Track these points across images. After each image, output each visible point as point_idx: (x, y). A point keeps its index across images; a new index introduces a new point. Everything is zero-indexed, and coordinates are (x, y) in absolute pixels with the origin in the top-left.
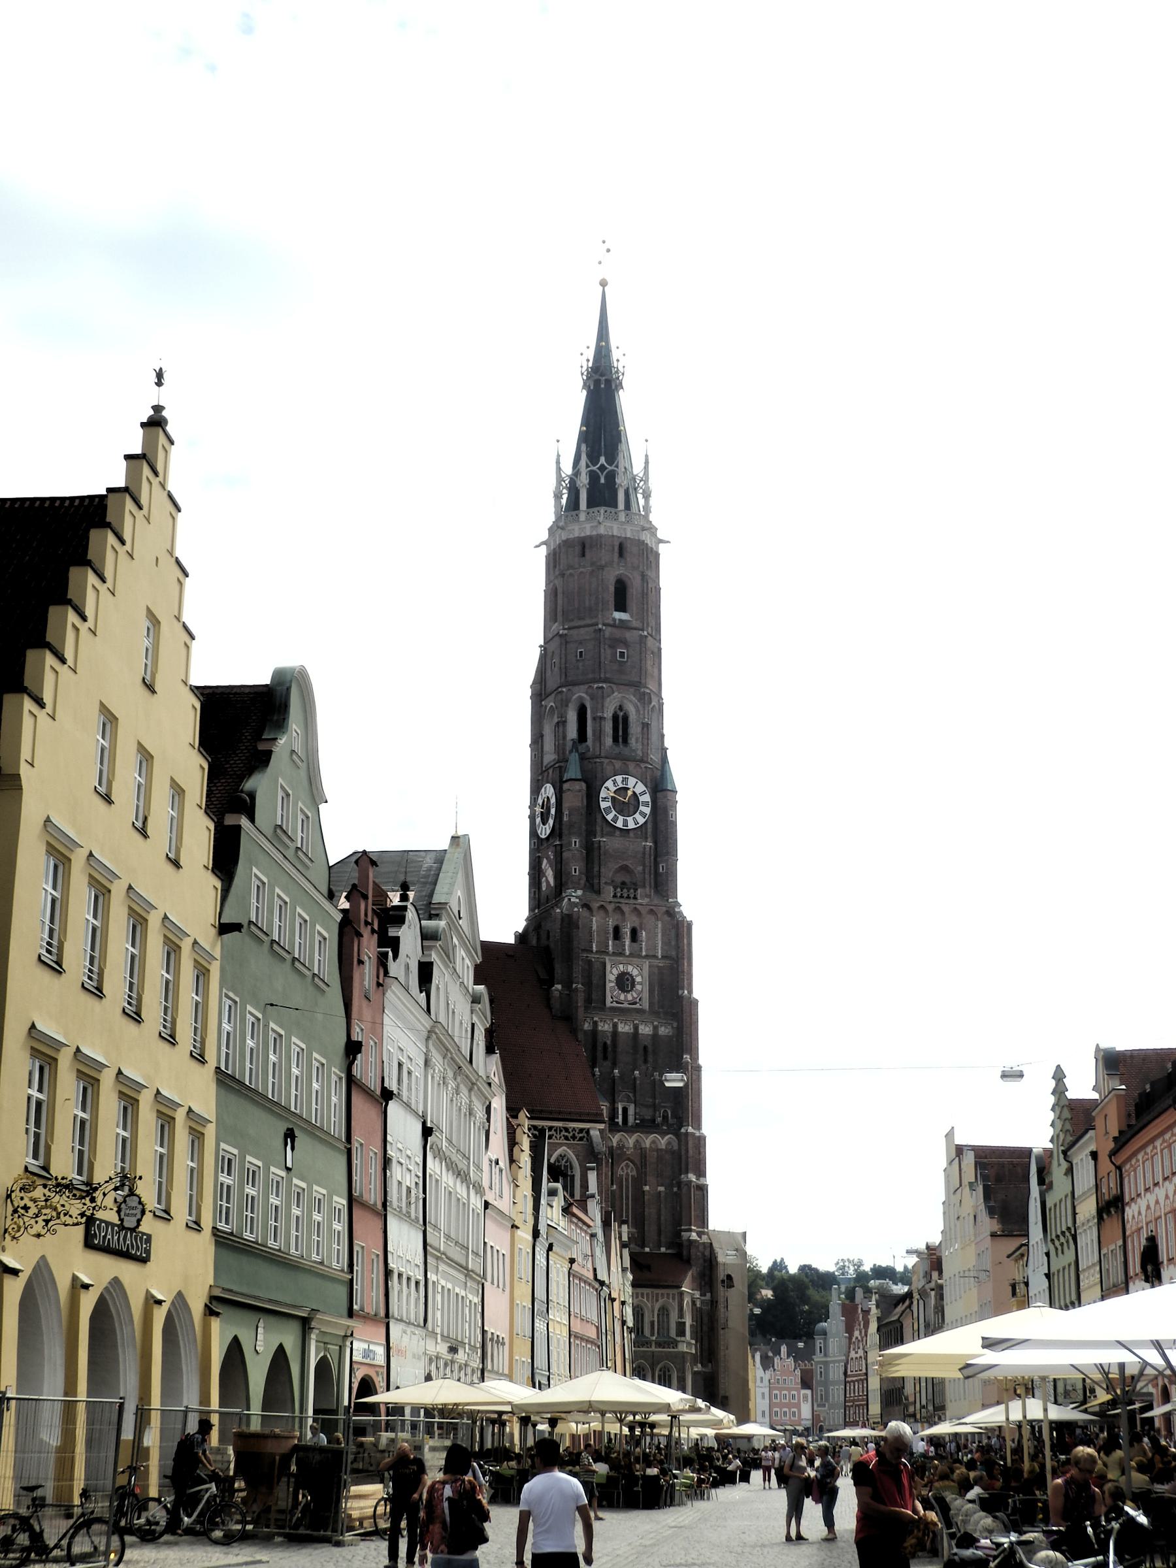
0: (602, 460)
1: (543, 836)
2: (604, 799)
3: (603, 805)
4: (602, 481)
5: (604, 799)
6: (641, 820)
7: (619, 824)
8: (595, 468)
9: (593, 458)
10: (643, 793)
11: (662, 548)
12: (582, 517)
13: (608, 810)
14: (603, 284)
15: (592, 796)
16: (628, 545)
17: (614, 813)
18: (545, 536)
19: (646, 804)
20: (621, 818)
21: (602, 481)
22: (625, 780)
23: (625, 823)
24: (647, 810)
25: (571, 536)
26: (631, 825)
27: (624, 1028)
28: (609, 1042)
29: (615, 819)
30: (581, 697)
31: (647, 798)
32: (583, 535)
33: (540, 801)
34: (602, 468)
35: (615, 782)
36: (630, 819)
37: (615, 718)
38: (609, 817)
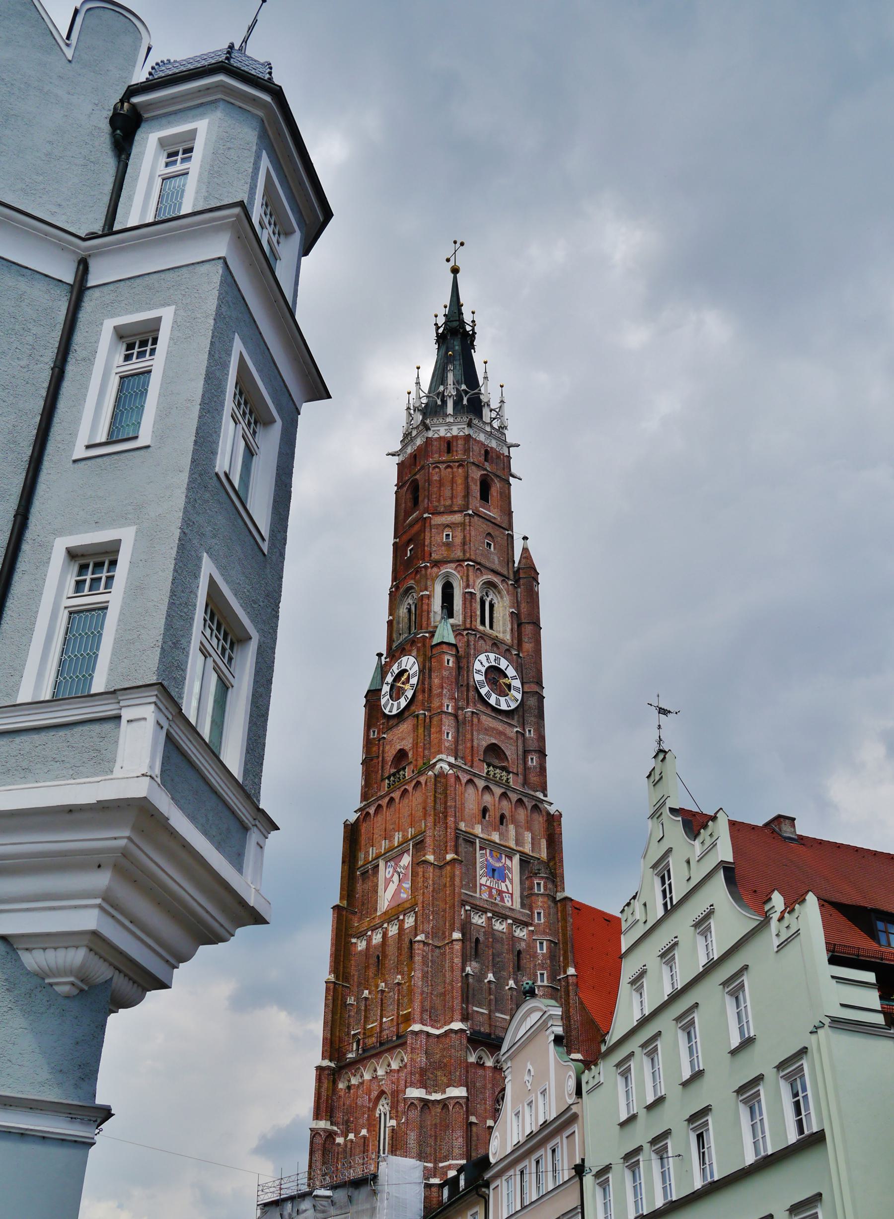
0: (464, 387)
1: (395, 712)
2: (478, 672)
4: (465, 402)
6: (513, 706)
7: (492, 701)
9: (457, 383)
10: (514, 678)
11: (511, 480)
12: (450, 419)
18: (399, 447)
21: (465, 402)
25: (436, 436)
26: (504, 707)
27: (500, 926)
28: (482, 939)
29: (488, 695)
30: (447, 575)
31: (517, 683)
32: (449, 435)
33: (389, 679)
34: (466, 393)
36: (502, 699)
38: (483, 691)
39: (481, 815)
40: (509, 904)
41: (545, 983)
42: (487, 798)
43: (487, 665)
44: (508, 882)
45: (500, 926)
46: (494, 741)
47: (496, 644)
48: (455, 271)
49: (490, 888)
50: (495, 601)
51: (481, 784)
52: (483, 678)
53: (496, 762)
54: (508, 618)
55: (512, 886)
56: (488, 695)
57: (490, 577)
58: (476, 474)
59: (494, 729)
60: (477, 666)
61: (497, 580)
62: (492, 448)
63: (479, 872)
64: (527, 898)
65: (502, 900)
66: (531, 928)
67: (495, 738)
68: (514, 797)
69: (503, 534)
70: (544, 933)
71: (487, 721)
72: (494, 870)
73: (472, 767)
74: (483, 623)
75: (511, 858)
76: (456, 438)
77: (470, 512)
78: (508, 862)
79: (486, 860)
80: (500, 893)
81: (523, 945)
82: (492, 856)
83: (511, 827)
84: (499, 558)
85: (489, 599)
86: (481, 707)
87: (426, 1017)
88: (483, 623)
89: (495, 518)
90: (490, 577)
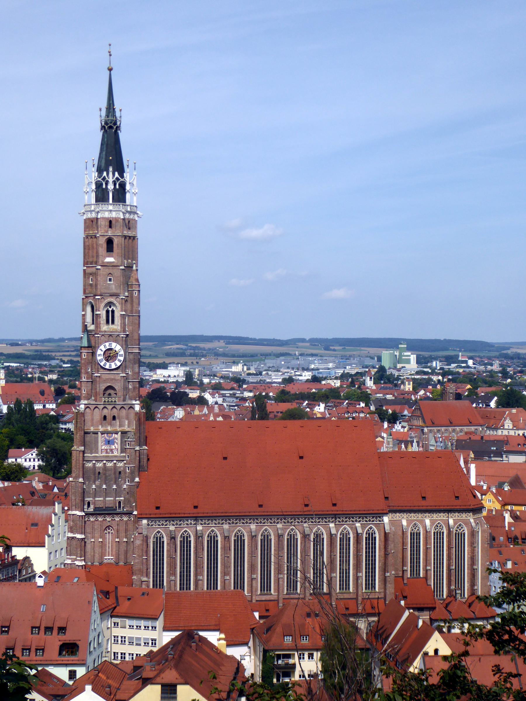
2: (99, 355)
3: (99, 358)
5: (99, 355)
6: (119, 364)
7: (107, 367)
8: (100, 179)
13: (101, 361)
14: (110, 70)
15: (93, 354)
16: (113, 222)
17: (104, 361)
19: (121, 356)
20: (108, 364)
22: (110, 345)
23: (110, 366)
24: (122, 358)
27: (110, 465)
31: (122, 352)
35: (105, 346)
38: (102, 364)
39: (103, 419)
40: (115, 454)
41: (129, 484)
42: (105, 411)
43: (104, 350)
44: (116, 445)
45: (110, 465)
46: (109, 385)
47: (111, 337)
48: (110, 70)
49: (107, 450)
50: (114, 309)
51: (101, 407)
52: (102, 357)
53: (111, 392)
54: (119, 318)
55: (117, 446)
56: (105, 365)
58: (102, 241)
59: (108, 379)
60: (99, 352)
62: (113, 218)
63: (100, 444)
64: (123, 450)
65: (113, 453)
66: (125, 462)
67: (109, 383)
68: (119, 407)
69: (118, 269)
70: (129, 464)
71: (106, 376)
72: (109, 441)
73: (96, 401)
74: (108, 322)
75: (117, 433)
76: (94, 218)
77: (99, 267)
78: (116, 436)
79: (105, 438)
80: (112, 450)
81: (122, 469)
82: (108, 436)
83: (117, 421)
84: (115, 285)
85: (110, 309)
86: (102, 371)
87: (74, 508)
89: (113, 262)
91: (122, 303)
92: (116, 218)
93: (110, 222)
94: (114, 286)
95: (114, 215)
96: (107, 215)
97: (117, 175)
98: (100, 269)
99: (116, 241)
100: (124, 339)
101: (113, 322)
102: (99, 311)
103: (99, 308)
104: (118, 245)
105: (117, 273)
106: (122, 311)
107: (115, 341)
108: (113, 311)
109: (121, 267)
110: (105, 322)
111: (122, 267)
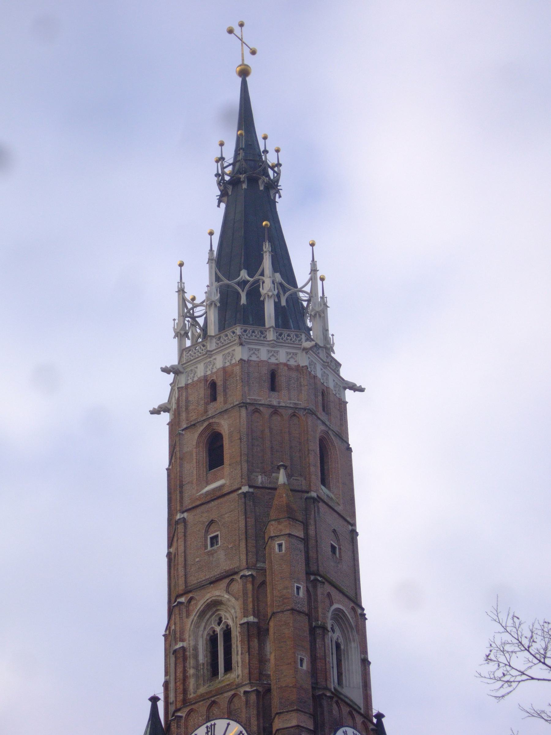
16: (219, 383)
37: (213, 639)
50: (230, 622)
57: (208, 596)
61: (217, 592)
88: (215, 672)
90: (208, 596)
91: (245, 593)
92: (224, 369)
93: (213, 386)
94: (221, 555)
95: (219, 362)
96: (201, 371)
97: (244, 274)
98: (184, 520)
99: (225, 426)
100: (253, 697)
101: (228, 668)
102: (182, 640)
103: (182, 632)
104: (231, 434)
105: (230, 513)
106: (245, 616)
107: (231, 715)
108: (227, 634)
109: (240, 491)
110: (206, 671)
111: (245, 489)
